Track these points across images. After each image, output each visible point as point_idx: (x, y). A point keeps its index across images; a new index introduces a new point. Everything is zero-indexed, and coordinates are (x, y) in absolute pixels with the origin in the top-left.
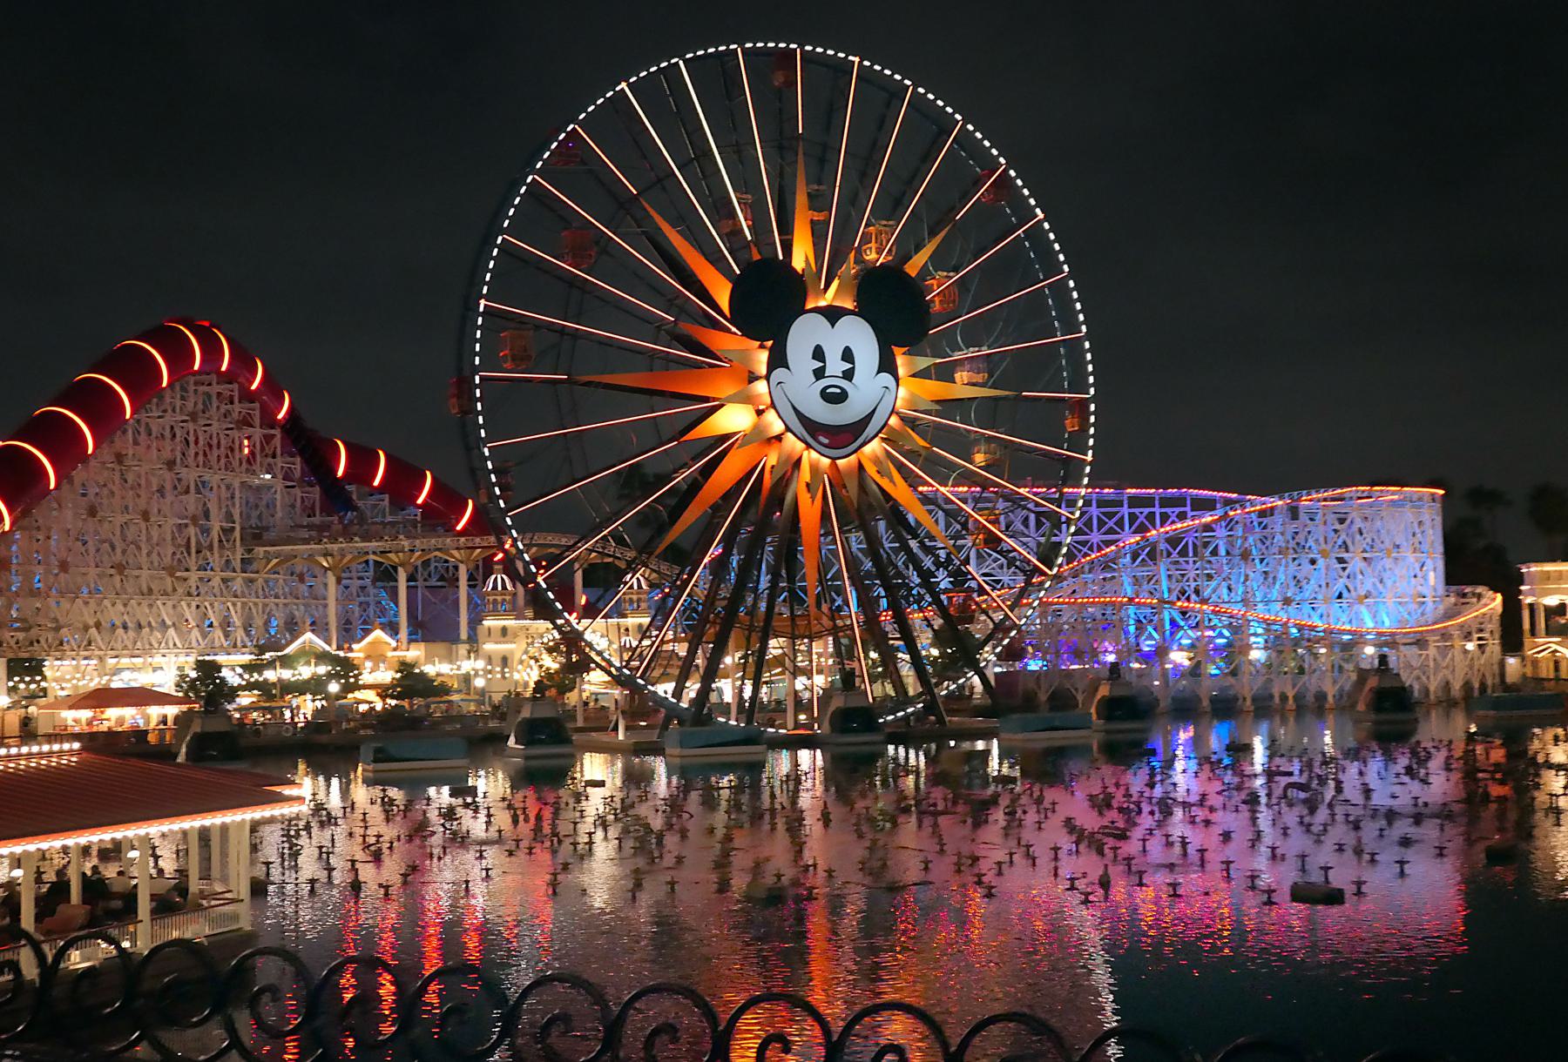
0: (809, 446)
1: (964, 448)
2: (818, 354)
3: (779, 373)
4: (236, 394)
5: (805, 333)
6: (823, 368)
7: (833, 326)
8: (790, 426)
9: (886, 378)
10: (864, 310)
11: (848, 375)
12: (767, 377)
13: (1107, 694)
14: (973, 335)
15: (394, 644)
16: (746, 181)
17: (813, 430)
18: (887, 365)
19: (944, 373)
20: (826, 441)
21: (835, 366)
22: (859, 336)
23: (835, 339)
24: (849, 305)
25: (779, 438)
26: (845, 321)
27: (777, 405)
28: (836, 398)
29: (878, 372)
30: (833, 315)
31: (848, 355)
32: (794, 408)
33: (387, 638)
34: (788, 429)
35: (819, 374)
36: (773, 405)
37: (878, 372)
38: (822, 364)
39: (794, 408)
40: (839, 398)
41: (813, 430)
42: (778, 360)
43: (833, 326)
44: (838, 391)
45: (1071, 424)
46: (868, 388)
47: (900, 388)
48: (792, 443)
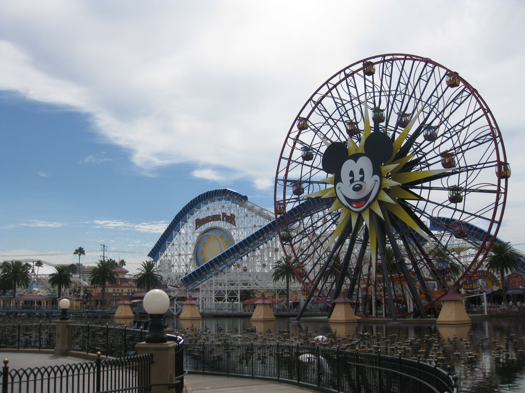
2: (352, 174)
3: (339, 185)
6: (353, 179)
9: (377, 177)
11: (362, 179)
18: (377, 171)
20: (355, 206)
21: (357, 177)
24: (364, 152)
29: (373, 176)
30: (355, 157)
31: (362, 172)
32: (343, 194)
35: (352, 181)
37: (373, 176)
38: (352, 178)
39: (343, 194)
42: (338, 179)
44: (359, 186)
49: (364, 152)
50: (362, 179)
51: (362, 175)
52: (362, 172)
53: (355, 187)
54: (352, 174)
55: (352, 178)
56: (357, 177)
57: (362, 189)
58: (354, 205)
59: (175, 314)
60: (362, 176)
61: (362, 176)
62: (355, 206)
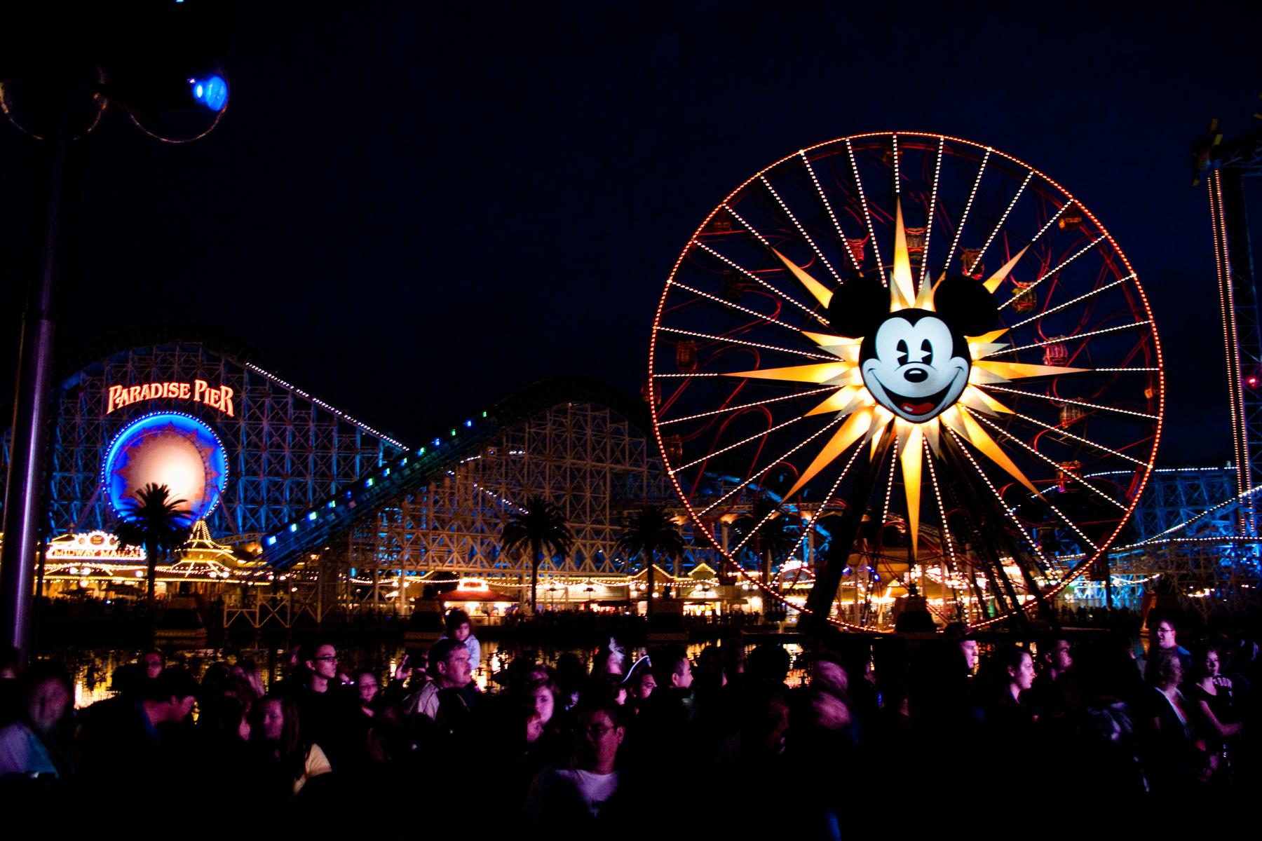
0: (896, 414)
1: (1051, 414)
2: (902, 346)
3: (870, 363)
4: (608, 416)
5: (890, 333)
7: (913, 323)
8: (880, 399)
9: (960, 361)
10: (943, 311)
11: (927, 360)
12: (861, 364)
13: (1154, 607)
14: (1052, 326)
15: (715, 573)
16: (856, 230)
17: (898, 401)
18: (961, 350)
19: (1034, 357)
20: (910, 410)
21: (916, 354)
22: (937, 332)
23: (914, 335)
25: (872, 408)
26: (924, 322)
27: (869, 385)
28: (916, 377)
29: (953, 356)
30: (913, 316)
31: (926, 346)
33: (709, 569)
34: (878, 402)
35: (903, 361)
36: (866, 385)
37: (953, 356)
38: (903, 354)
40: (922, 376)
41: (898, 401)
42: (868, 351)
43: (913, 323)
44: (919, 372)
45: (1148, 394)
46: (944, 366)
47: (973, 368)
48: (885, 416)
49: (928, 306)
50: (927, 360)
51: (928, 353)
52: (926, 346)
53: (912, 372)
54: (902, 346)
55: (903, 354)
56: (916, 354)
57: (926, 381)
58: (906, 408)
59: (257, 626)
60: (928, 353)
61: (926, 354)
62: (910, 410)
